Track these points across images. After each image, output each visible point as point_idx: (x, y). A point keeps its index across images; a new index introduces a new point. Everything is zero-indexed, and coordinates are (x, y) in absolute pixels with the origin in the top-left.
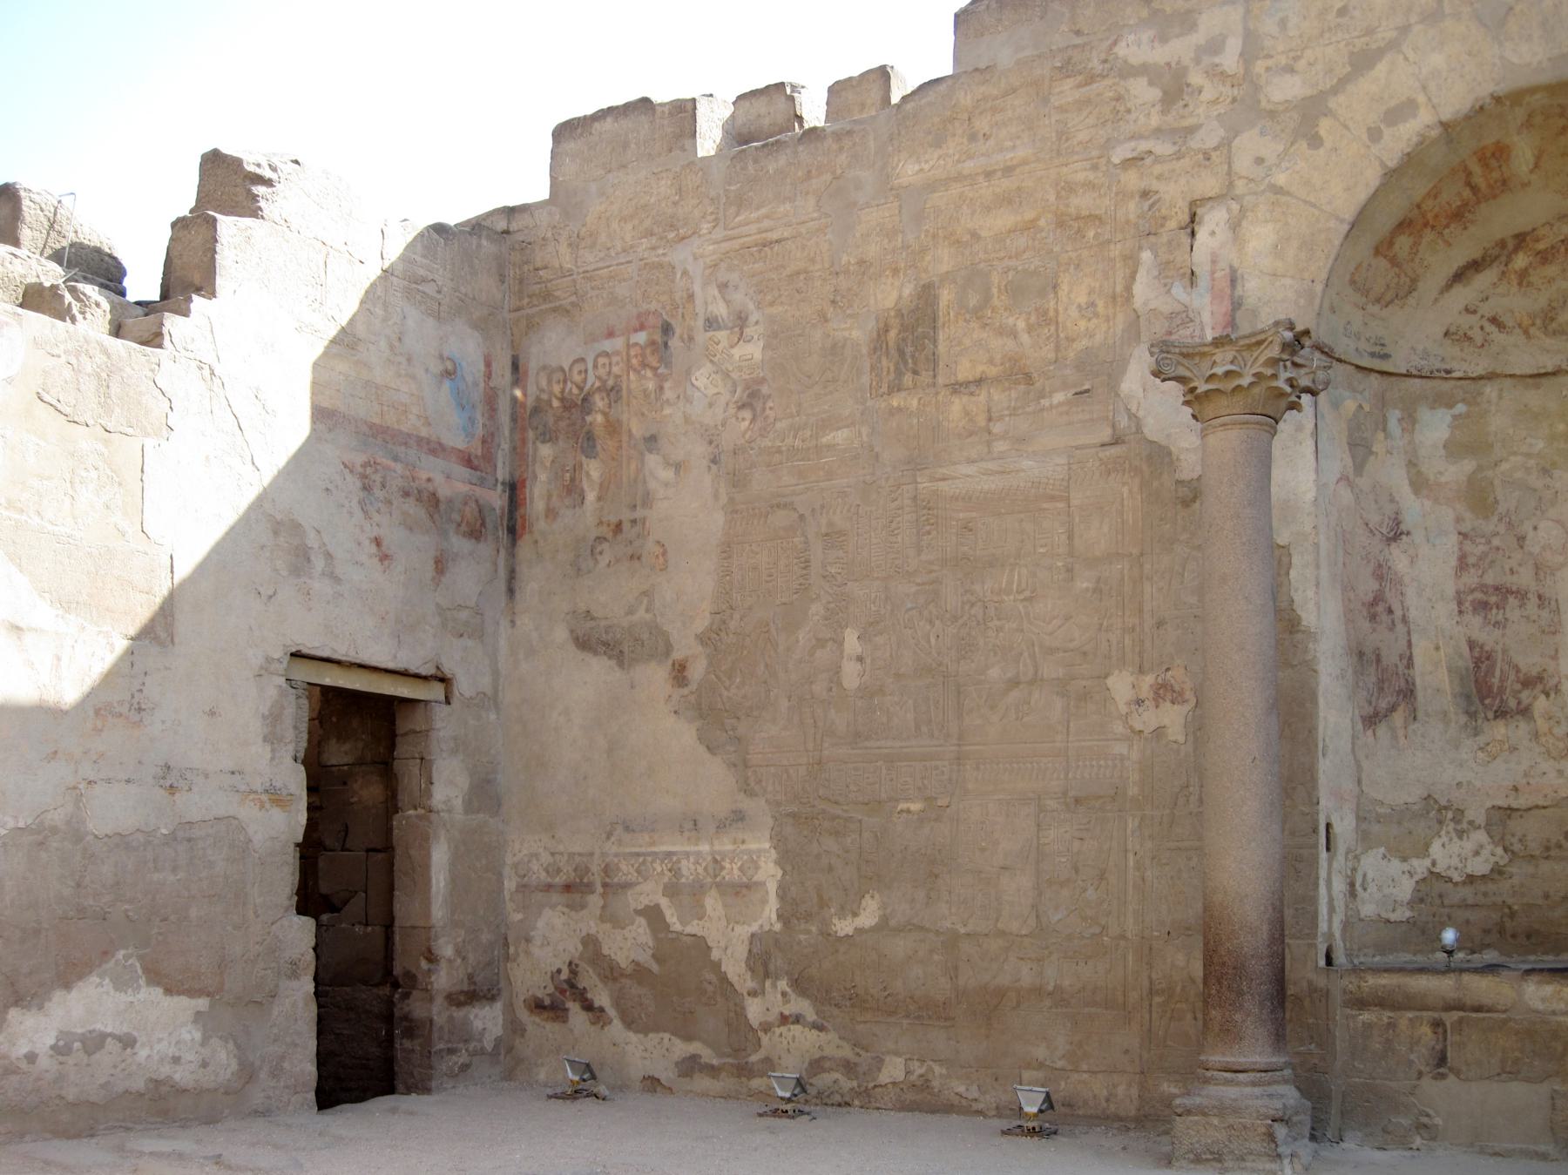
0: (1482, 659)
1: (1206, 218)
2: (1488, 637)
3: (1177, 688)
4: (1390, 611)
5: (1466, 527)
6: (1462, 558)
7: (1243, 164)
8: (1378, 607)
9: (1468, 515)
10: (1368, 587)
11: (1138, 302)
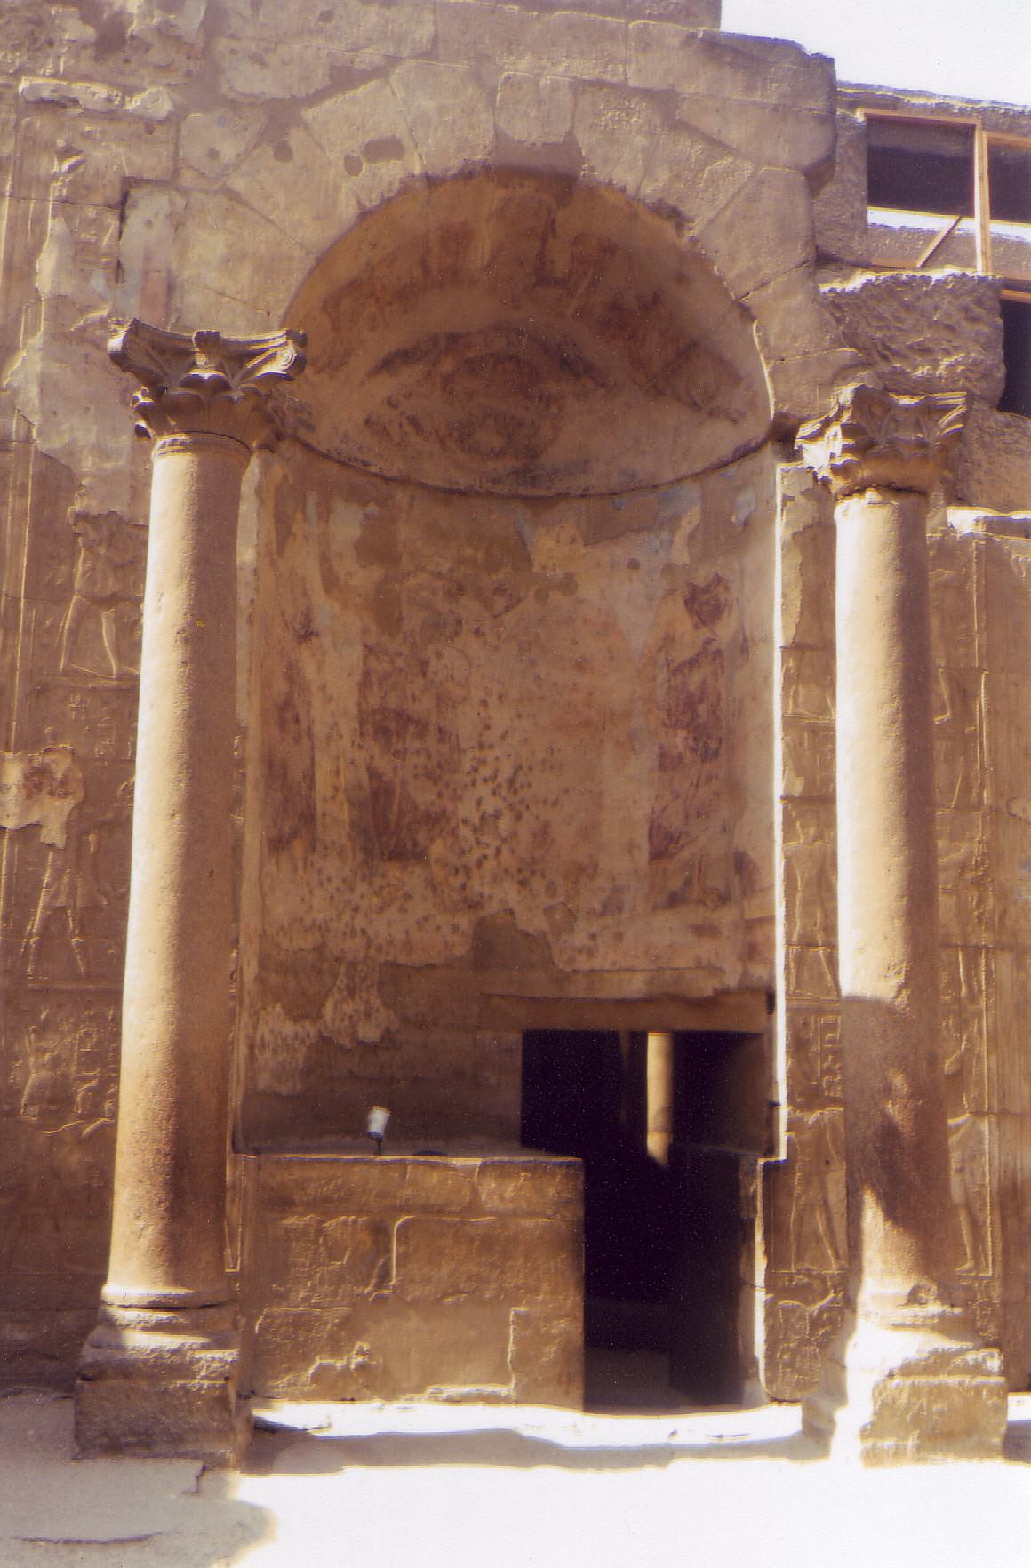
4: (297, 721)
6: (367, 674)
9: (373, 628)
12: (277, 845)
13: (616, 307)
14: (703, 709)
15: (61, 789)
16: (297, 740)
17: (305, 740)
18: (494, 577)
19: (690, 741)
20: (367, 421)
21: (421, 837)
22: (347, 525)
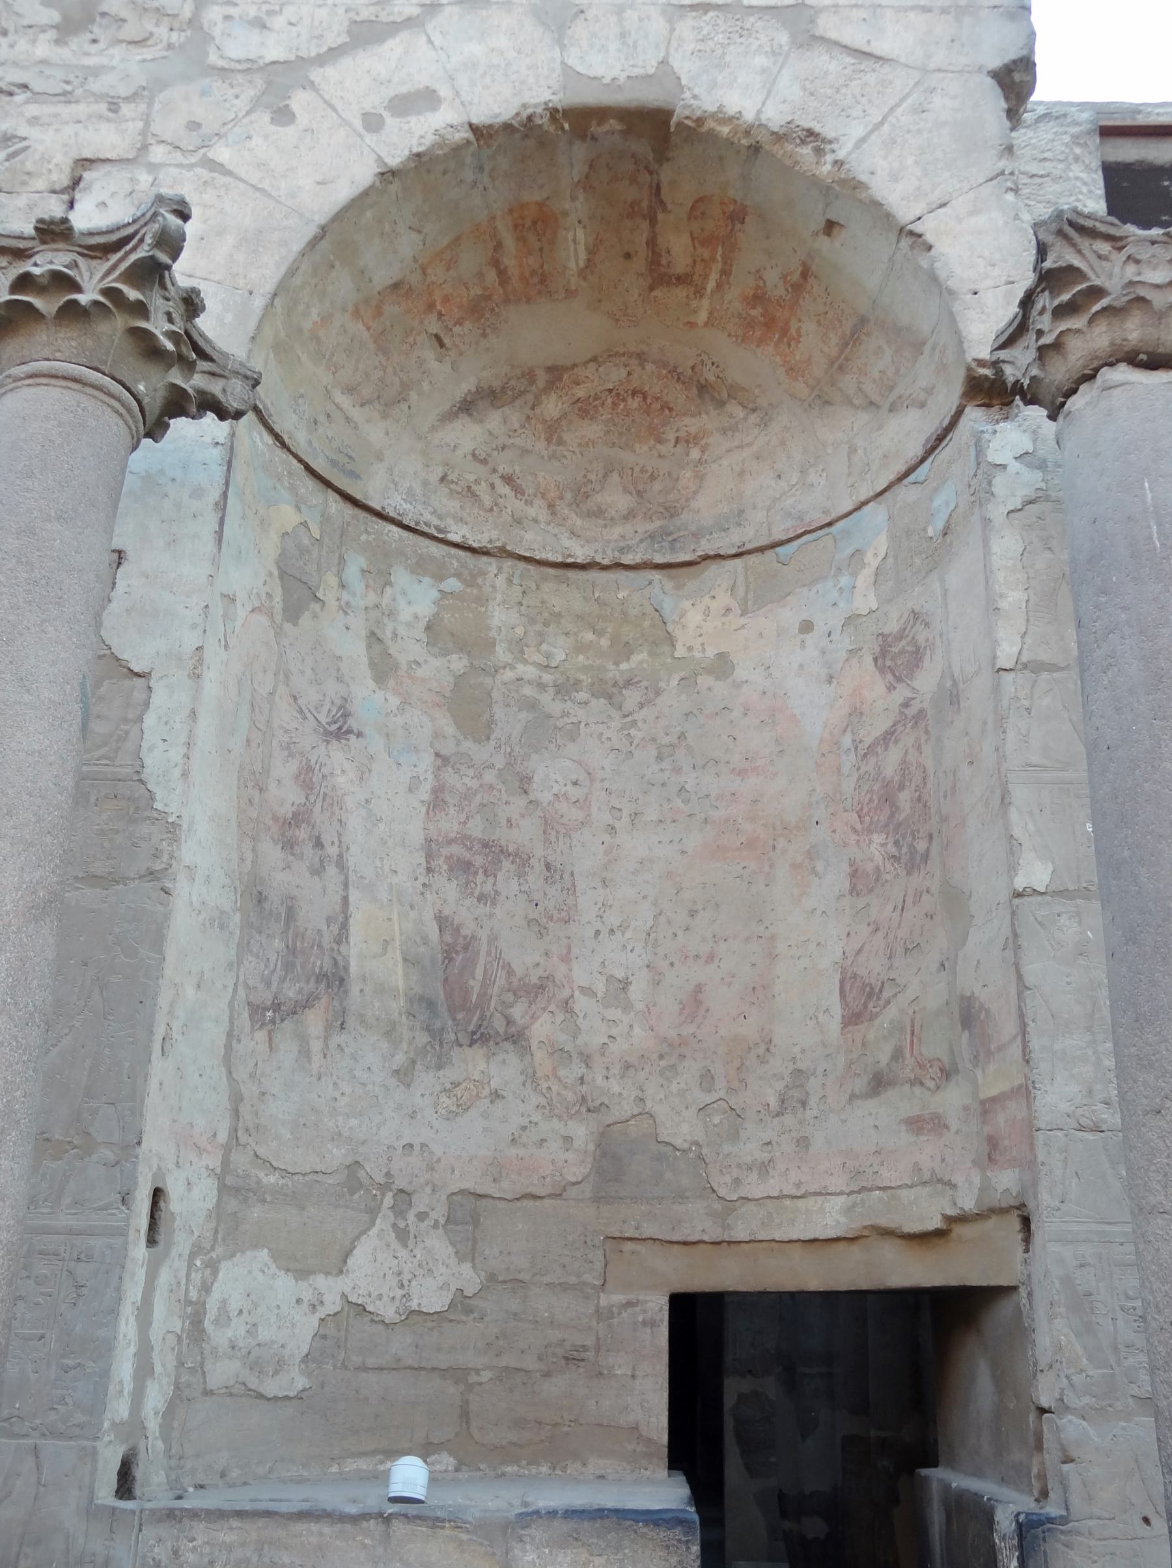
0: (455, 948)
2: (466, 913)
4: (319, 844)
5: (447, 748)
6: (438, 791)
7: (168, 126)
9: (450, 729)
10: (286, 796)
12: (271, 1013)
13: (758, 298)
16: (317, 871)
17: (332, 870)
18: (624, 666)
19: (893, 850)
20: (443, 479)
22: (416, 599)
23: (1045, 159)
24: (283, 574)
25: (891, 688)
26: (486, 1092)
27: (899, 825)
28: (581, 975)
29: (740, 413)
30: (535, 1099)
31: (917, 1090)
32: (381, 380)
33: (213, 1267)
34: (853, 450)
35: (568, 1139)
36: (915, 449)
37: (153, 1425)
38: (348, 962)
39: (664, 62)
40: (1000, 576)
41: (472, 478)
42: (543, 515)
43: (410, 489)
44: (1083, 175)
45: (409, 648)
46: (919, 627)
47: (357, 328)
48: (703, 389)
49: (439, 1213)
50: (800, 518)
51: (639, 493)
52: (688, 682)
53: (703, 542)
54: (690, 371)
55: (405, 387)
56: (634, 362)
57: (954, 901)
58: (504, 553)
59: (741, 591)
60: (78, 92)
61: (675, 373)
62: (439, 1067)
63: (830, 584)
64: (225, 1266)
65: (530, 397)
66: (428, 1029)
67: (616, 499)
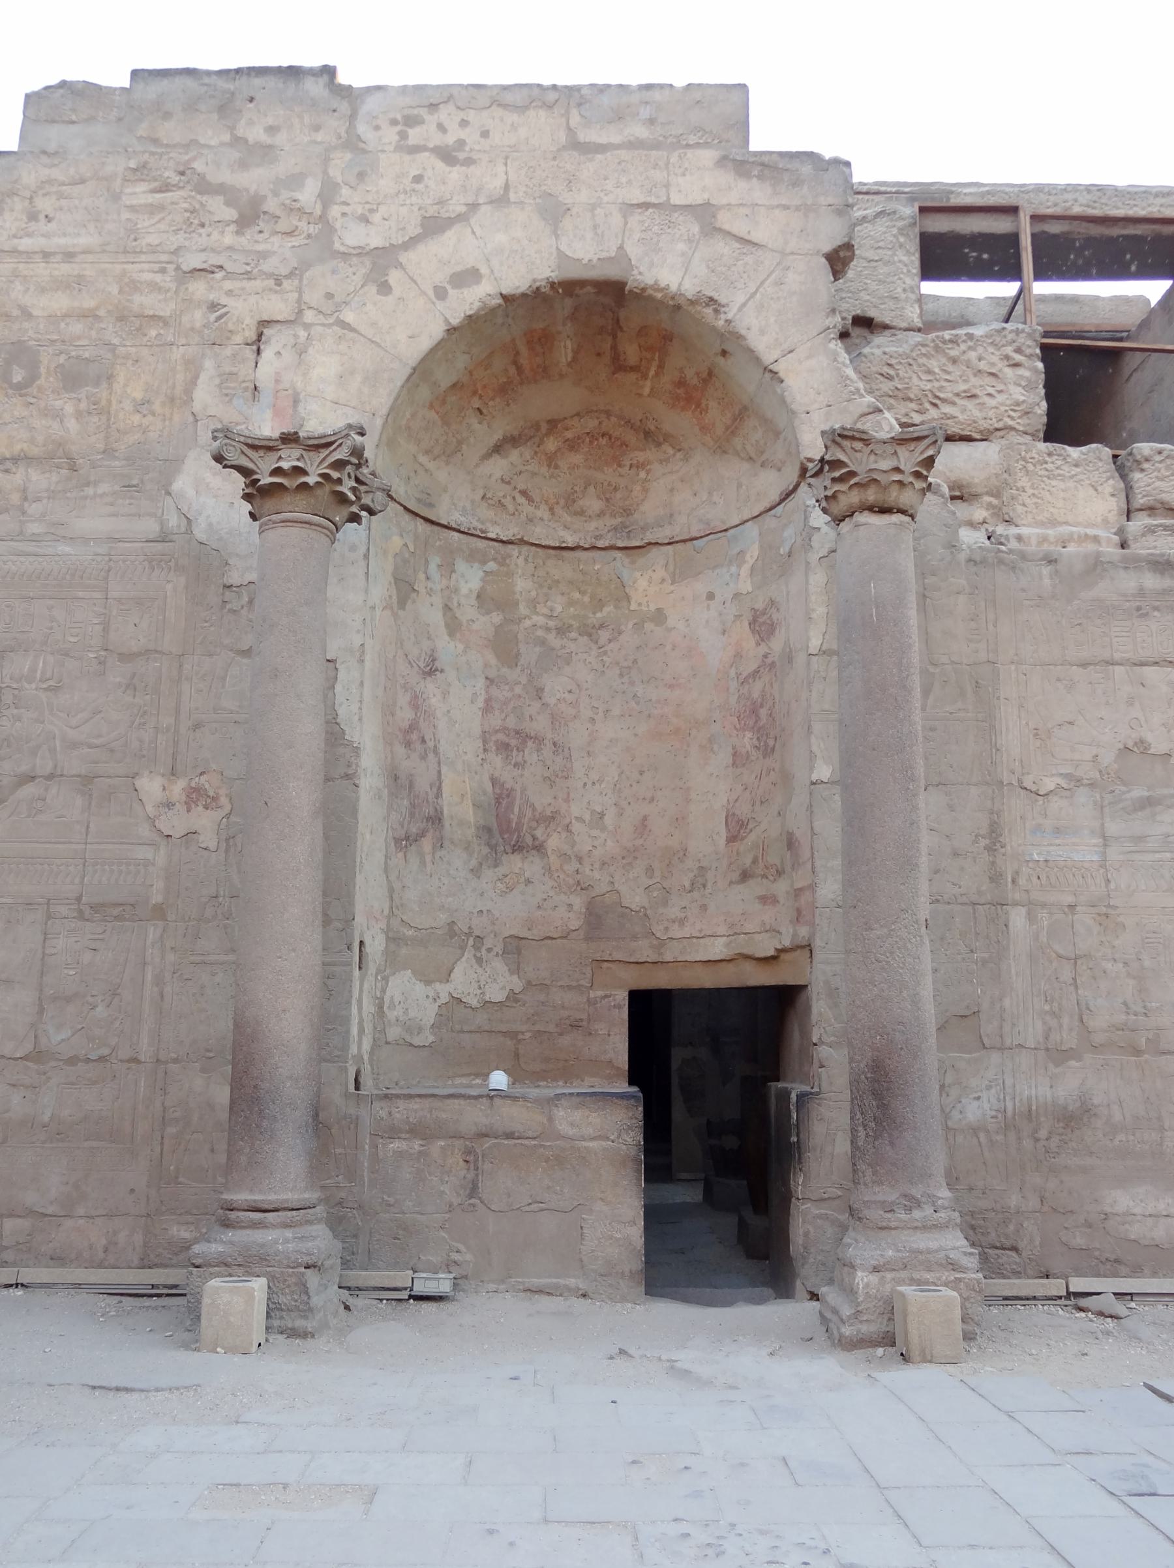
0: (502, 797)
1: (273, 341)
2: (507, 776)
3: (211, 794)
4: (424, 741)
5: (492, 673)
6: (488, 701)
7: (313, 297)
8: (412, 735)
9: (493, 661)
10: (405, 715)
11: (197, 406)
12: (405, 841)
14: (763, 712)
15: (212, 802)
16: (424, 757)
17: (431, 756)
18: (599, 615)
19: (756, 743)
20: (483, 497)
21: (539, 833)
22: (470, 578)
23: (879, 248)
24: (396, 579)
25: (758, 644)
26: (522, 880)
27: (759, 729)
28: (575, 810)
29: (671, 451)
30: (551, 883)
31: (765, 881)
32: (446, 441)
33: (386, 979)
34: (739, 486)
35: (570, 905)
36: (775, 496)
37: (366, 1057)
38: (442, 808)
39: (621, 248)
40: (813, 598)
41: (501, 494)
42: (546, 515)
43: (464, 508)
44: (905, 259)
45: (468, 612)
46: (774, 610)
47: (432, 415)
48: (647, 434)
49: (499, 949)
50: (708, 524)
51: (607, 500)
52: (639, 627)
53: (648, 533)
54: (638, 423)
55: (460, 443)
56: (603, 417)
57: (786, 778)
58: (522, 542)
59: (671, 568)
60: (255, 271)
61: (629, 423)
62: (496, 866)
63: (725, 570)
64: (391, 979)
65: (536, 440)
66: (488, 844)
67: (593, 503)
